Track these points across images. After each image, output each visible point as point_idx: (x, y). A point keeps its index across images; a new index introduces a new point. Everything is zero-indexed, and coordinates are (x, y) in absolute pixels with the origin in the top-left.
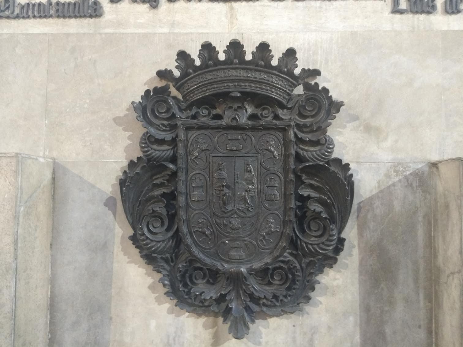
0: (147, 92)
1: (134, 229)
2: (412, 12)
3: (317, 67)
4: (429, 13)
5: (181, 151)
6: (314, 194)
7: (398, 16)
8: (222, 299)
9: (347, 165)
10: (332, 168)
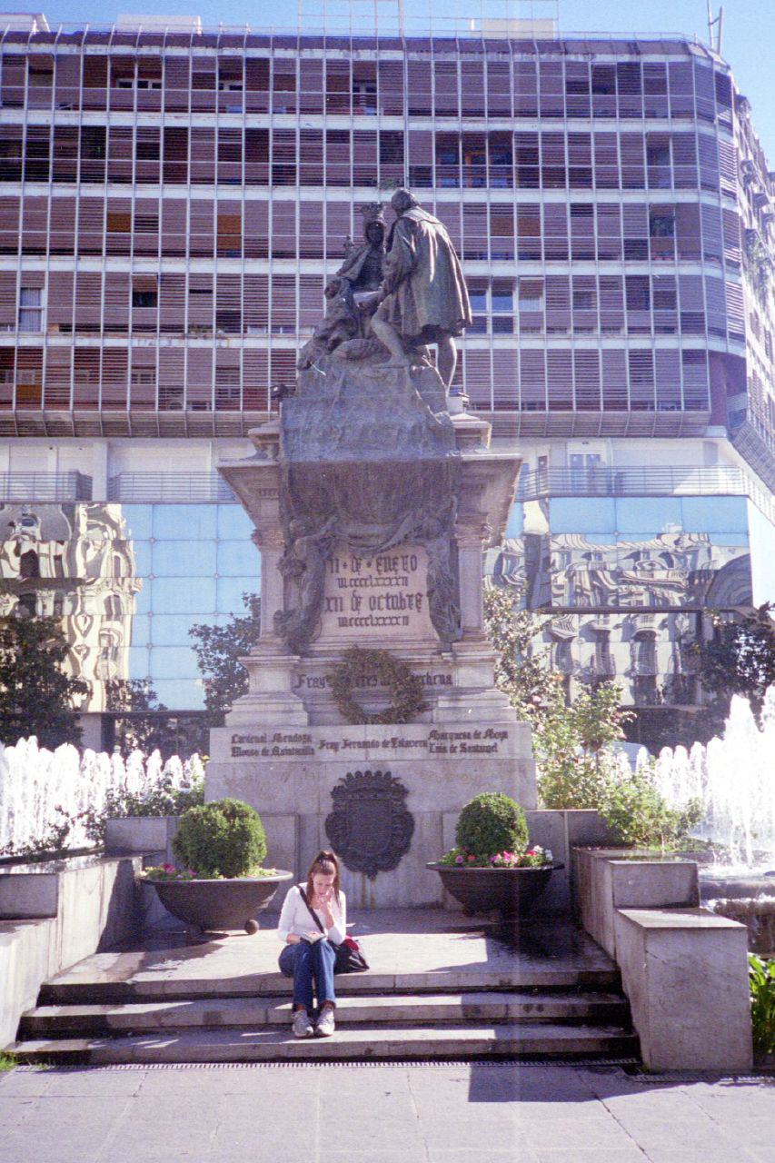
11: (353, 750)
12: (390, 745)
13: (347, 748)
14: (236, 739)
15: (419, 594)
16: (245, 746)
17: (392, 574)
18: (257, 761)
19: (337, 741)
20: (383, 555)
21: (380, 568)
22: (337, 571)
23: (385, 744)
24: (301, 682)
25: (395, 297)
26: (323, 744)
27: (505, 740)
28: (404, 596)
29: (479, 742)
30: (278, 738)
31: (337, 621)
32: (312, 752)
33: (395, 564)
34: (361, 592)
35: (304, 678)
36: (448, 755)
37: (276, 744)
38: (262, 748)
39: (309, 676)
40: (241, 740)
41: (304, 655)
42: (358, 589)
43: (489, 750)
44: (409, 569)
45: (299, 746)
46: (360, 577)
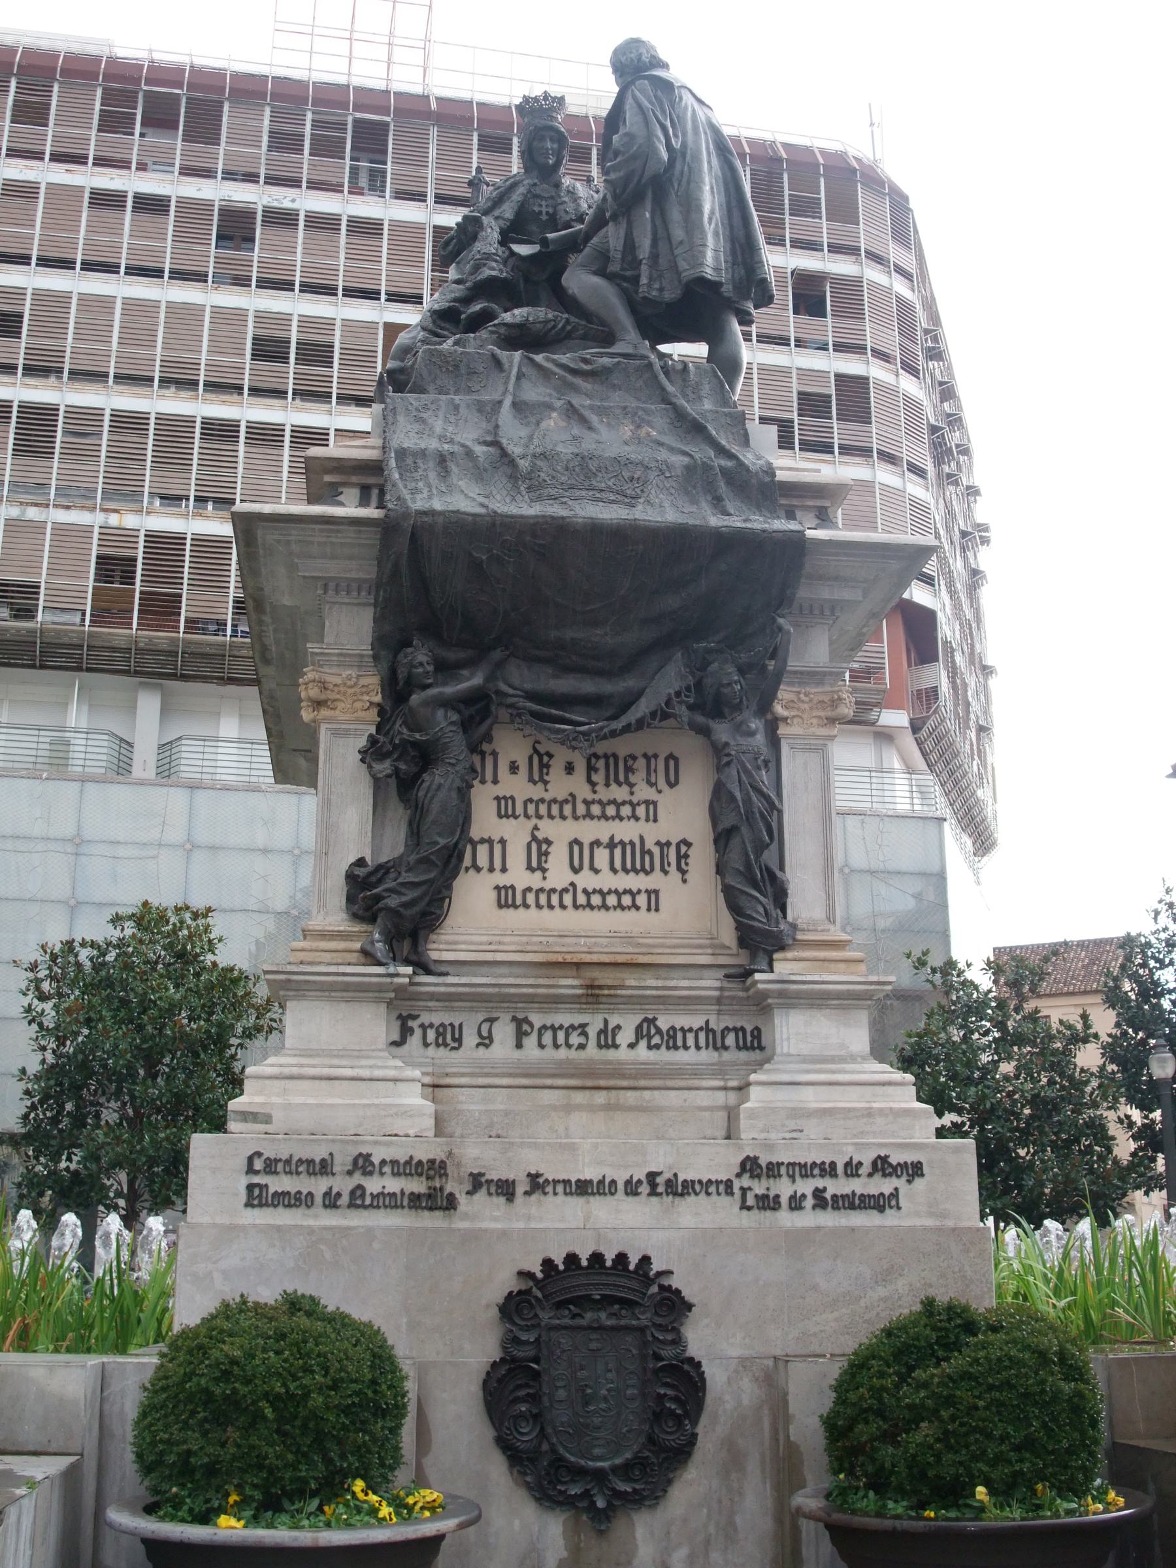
0: (511, 1293)
1: (497, 1430)
3: (670, 1268)
4: (774, 1209)
5: (545, 1352)
6: (669, 1392)
7: (745, 1212)
8: (586, 1494)
9: (699, 1363)
10: (686, 1367)
11: (550, 1198)
12: (645, 1189)
14: (258, 1165)
16: (278, 1184)
17: (620, 793)
18: (311, 1222)
19: (511, 1177)
20: (601, 748)
22: (495, 781)
23: (631, 1188)
24: (406, 1032)
26: (477, 1182)
27: (918, 1182)
28: (650, 844)
29: (858, 1186)
30: (363, 1164)
31: (494, 894)
32: (450, 1204)
33: (629, 770)
34: (547, 828)
35: (410, 1023)
36: (785, 1218)
37: (358, 1179)
38: (324, 1189)
39: (425, 1018)
40: (271, 1167)
41: (423, 967)
42: (541, 824)
43: (879, 1203)
45: (418, 1186)
46: (548, 796)
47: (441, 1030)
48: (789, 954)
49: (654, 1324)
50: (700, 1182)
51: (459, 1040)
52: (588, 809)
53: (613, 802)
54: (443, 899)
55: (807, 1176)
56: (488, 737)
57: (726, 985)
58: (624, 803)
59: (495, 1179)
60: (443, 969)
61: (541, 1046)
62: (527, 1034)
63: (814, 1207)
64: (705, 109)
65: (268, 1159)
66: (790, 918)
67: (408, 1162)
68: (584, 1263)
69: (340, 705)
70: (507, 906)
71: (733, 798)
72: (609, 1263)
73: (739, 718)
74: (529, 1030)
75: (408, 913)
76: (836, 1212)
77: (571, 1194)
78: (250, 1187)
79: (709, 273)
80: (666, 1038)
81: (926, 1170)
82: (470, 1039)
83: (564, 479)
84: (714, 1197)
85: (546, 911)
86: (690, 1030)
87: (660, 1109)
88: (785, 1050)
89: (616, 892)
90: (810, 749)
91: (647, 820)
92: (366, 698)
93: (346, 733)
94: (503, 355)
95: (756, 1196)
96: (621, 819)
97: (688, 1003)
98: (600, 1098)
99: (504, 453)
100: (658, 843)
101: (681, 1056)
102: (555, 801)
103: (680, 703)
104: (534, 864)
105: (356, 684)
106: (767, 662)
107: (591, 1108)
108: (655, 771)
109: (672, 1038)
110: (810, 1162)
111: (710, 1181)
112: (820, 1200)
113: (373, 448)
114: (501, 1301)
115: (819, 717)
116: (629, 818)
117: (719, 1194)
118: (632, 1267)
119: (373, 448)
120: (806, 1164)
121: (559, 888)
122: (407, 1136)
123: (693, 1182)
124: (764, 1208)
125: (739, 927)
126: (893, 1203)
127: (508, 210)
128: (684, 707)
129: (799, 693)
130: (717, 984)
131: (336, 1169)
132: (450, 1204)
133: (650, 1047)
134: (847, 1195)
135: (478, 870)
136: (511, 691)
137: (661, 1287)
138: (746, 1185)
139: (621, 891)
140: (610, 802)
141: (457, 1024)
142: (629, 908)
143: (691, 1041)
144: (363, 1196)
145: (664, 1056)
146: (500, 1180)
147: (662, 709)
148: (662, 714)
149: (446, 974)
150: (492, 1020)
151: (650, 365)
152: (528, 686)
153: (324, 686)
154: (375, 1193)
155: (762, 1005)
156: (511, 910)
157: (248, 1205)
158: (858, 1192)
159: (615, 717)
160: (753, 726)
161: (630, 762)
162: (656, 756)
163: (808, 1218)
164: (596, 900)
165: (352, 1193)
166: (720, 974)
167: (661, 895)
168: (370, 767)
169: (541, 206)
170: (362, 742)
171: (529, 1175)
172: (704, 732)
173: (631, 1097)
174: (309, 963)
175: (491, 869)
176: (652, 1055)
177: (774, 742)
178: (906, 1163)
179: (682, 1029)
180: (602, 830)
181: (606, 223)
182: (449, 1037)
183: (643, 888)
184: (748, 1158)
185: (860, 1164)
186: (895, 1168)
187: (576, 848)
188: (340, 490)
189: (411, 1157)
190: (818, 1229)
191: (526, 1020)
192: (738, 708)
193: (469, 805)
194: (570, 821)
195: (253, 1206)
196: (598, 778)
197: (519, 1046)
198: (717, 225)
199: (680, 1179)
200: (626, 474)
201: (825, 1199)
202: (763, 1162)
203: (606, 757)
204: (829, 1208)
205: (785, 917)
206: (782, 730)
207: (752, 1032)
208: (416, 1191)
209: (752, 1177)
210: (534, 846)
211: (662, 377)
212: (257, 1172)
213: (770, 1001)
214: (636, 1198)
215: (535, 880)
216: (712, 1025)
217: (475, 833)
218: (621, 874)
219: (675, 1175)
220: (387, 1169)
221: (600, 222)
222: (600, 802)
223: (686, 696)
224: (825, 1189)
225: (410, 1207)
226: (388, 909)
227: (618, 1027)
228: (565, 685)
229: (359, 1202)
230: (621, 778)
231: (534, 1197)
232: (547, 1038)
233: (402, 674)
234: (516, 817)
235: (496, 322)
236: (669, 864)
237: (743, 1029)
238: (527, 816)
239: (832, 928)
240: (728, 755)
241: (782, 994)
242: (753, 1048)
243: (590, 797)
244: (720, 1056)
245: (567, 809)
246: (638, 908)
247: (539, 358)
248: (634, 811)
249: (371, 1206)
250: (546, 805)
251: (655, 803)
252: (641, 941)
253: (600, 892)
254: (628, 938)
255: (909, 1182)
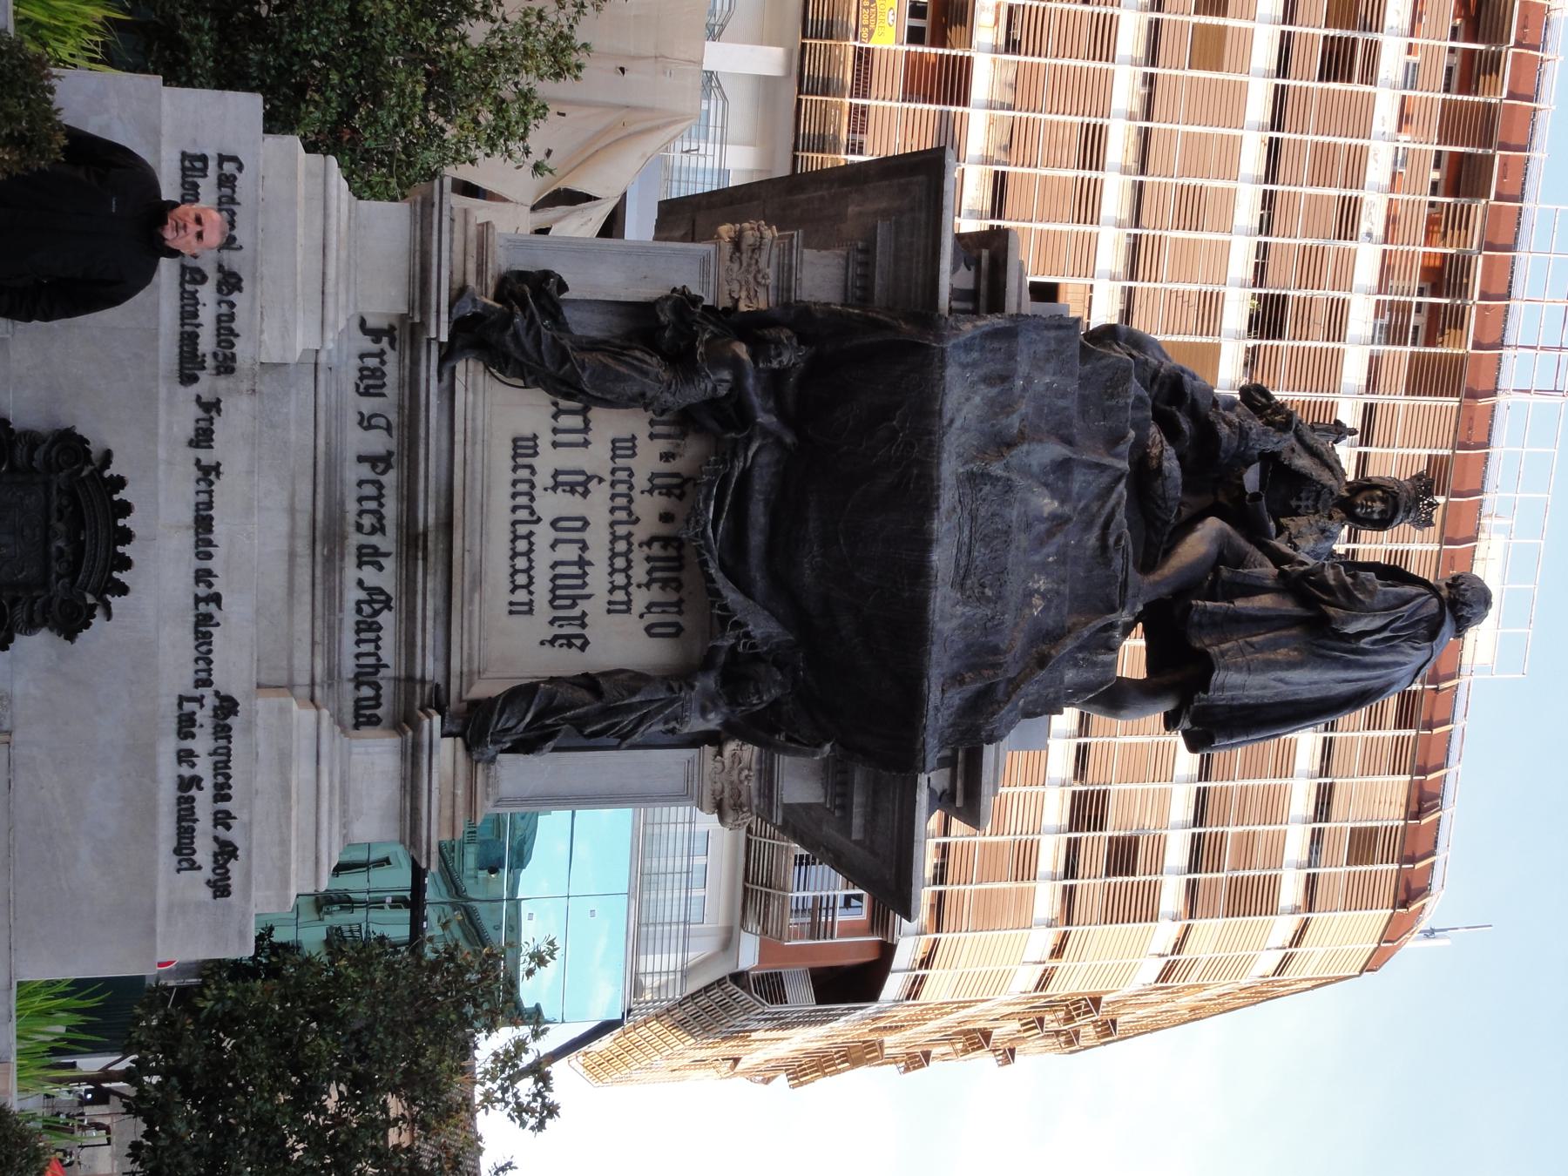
0: (87, 442)
2: (180, 717)
3: (114, 617)
4: (179, 733)
7: (175, 701)
9: (7, 649)
11: (192, 487)
12: (202, 590)
13: (197, 474)
15: (586, 643)
17: (639, 572)
21: (656, 546)
22: (652, 436)
23: (203, 576)
24: (376, 334)
25: (1269, 582)
26: (211, 407)
27: (207, 893)
28: (583, 605)
30: (230, 282)
31: (528, 433)
33: (665, 583)
34: (600, 494)
35: (385, 340)
36: (169, 745)
37: (213, 277)
39: (391, 357)
40: (226, 181)
41: (448, 354)
42: (606, 485)
44: (651, 618)
45: (207, 342)
46: (635, 494)
47: (377, 373)
48: (461, 754)
49: (52, 598)
50: (210, 651)
51: (366, 393)
52: (621, 538)
53: (629, 566)
54: (523, 378)
55: (216, 769)
56: (701, 430)
57: (427, 688)
58: (628, 577)
59: (214, 427)
60: (446, 377)
61: (360, 483)
62: (374, 467)
63: (180, 777)
64: (1410, 677)
65: (235, 178)
66: (501, 757)
67: (232, 332)
68: (121, 522)
69: (736, 266)
70: (515, 448)
71: (633, 693)
72: (120, 549)
73: (721, 703)
74: (378, 470)
75: (508, 338)
76: (175, 801)
77: (197, 510)
78: (204, 159)
79: (1218, 677)
80: (369, 620)
81: (220, 900)
82: (369, 405)
83: (982, 512)
84: (192, 667)
85: (510, 490)
86: (378, 648)
87: (291, 610)
88: (355, 750)
89: (531, 568)
90: (688, 780)
91: (610, 603)
92: (743, 294)
93: (704, 273)
94: (1124, 448)
95: (194, 713)
96: (611, 574)
97: (408, 645)
98: (303, 547)
99: (1010, 445)
100: (584, 614)
101: (349, 637)
102: (631, 501)
103: (738, 638)
104: (561, 478)
105: (758, 283)
106: (783, 734)
107: (292, 535)
108: (663, 612)
109: (367, 627)
110: (231, 772)
111: (210, 662)
112: (188, 784)
113: (1019, 305)
114: (79, 431)
115: (723, 791)
116: (612, 583)
117: (197, 672)
118: (116, 574)
119: (1019, 305)
120: (230, 768)
121: (535, 505)
122: (262, 332)
123: (210, 643)
124: (180, 722)
125: (491, 701)
126: (185, 865)
127: (1303, 462)
128: (732, 641)
129: (750, 769)
130: (428, 677)
131: (225, 253)
132: (188, 378)
133: (359, 603)
134: (193, 813)
135: (555, 417)
136: (750, 454)
137: (93, 607)
138: (205, 701)
139: (532, 573)
140: (629, 562)
141: (385, 391)
142: (513, 582)
143: (366, 648)
144: (194, 281)
145: (350, 618)
146: (212, 432)
147: (730, 617)
148: (725, 620)
149: (440, 380)
150: (388, 429)
151: (1113, 610)
152: (756, 472)
153: (756, 248)
154: (198, 295)
155: (405, 722)
156: (512, 453)
157: (184, 156)
158: (197, 826)
159: (723, 567)
160: (711, 716)
161: (674, 585)
162: (680, 613)
163: (168, 771)
164: (522, 546)
165: (198, 270)
166: (440, 680)
167: (528, 616)
168: (667, 298)
169: (1308, 499)
170: (695, 290)
171: (219, 464)
172: (707, 664)
173: (303, 579)
174: (451, 231)
175: (555, 431)
176: (350, 605)
177: (695, 741)
178: (229, 878)
179: (379, 638)
180: (598, 554)
181: (1277, 566)
182: (371, 382)
183: (534, 597)
184: (236, 704)
185: (228, 828)
186: (223, 866)
187: (579, 524)
188: (973, 268)
189: (237, 335)
190: (154, 781)
191: (388, 467)
192: (733, 702)
193: (627, 407)
194: (608, 518)
195: (182, 161)
196: (656, 549)
197: (361, 459)
198: (1274, 687)
199: (212, 629)
200: (987, 580)
201: (190, 789)
202: (232, 721)
203: (680, 558)
204: (179, 794)
205: (503, 751)
206: (709, 750)
207: (375, 715)
208: (200, 340)
209: (215, 709)
210: (581, 478)
211: (1099, 623)
212: (220, 166)
213: (410, 733)
214: (192, 581)
215: (543, 478)
216: (383, 672)
217: (597, 414)
218: (550, 574)
219: (218, 625)
220: (224, 309)
221: (1278, 558)
222: (630, 550)
223: (745, 644)
224: (200, 789)
225: (182, 334)
226: (512, 315)
227: (381, 568)
228: (758, 514)
229: (188, 277)
230: (657, 575)
231: (194, 469)
232: (369, 490)
233: (771, 333)
234: (613, 458)
235: (1165, 442)
236: (561, 626)
237: (378, 705)
238: (613, 472)
239: (490, 803)
240: (680, 690)
241: (416, 746)
242: (357, 715)
243: (635, 540)
244: (350, 680)
245: (621, 515)
246: (512, 591)
247: (1121, 486)
248: (620, 588)
249: (183, 291)
250: (626, 491)
251: (628, 611)
252: (477, 596)
253: (531, 550)
254: (478, 581)
255: (208, 882)
